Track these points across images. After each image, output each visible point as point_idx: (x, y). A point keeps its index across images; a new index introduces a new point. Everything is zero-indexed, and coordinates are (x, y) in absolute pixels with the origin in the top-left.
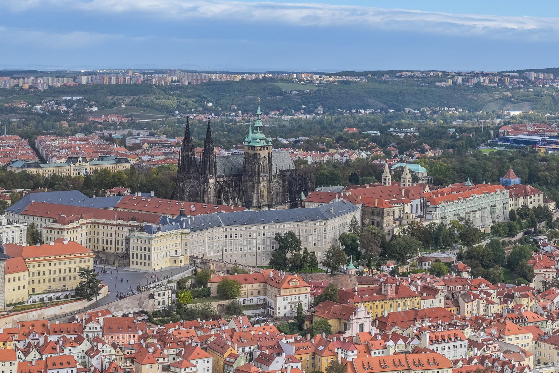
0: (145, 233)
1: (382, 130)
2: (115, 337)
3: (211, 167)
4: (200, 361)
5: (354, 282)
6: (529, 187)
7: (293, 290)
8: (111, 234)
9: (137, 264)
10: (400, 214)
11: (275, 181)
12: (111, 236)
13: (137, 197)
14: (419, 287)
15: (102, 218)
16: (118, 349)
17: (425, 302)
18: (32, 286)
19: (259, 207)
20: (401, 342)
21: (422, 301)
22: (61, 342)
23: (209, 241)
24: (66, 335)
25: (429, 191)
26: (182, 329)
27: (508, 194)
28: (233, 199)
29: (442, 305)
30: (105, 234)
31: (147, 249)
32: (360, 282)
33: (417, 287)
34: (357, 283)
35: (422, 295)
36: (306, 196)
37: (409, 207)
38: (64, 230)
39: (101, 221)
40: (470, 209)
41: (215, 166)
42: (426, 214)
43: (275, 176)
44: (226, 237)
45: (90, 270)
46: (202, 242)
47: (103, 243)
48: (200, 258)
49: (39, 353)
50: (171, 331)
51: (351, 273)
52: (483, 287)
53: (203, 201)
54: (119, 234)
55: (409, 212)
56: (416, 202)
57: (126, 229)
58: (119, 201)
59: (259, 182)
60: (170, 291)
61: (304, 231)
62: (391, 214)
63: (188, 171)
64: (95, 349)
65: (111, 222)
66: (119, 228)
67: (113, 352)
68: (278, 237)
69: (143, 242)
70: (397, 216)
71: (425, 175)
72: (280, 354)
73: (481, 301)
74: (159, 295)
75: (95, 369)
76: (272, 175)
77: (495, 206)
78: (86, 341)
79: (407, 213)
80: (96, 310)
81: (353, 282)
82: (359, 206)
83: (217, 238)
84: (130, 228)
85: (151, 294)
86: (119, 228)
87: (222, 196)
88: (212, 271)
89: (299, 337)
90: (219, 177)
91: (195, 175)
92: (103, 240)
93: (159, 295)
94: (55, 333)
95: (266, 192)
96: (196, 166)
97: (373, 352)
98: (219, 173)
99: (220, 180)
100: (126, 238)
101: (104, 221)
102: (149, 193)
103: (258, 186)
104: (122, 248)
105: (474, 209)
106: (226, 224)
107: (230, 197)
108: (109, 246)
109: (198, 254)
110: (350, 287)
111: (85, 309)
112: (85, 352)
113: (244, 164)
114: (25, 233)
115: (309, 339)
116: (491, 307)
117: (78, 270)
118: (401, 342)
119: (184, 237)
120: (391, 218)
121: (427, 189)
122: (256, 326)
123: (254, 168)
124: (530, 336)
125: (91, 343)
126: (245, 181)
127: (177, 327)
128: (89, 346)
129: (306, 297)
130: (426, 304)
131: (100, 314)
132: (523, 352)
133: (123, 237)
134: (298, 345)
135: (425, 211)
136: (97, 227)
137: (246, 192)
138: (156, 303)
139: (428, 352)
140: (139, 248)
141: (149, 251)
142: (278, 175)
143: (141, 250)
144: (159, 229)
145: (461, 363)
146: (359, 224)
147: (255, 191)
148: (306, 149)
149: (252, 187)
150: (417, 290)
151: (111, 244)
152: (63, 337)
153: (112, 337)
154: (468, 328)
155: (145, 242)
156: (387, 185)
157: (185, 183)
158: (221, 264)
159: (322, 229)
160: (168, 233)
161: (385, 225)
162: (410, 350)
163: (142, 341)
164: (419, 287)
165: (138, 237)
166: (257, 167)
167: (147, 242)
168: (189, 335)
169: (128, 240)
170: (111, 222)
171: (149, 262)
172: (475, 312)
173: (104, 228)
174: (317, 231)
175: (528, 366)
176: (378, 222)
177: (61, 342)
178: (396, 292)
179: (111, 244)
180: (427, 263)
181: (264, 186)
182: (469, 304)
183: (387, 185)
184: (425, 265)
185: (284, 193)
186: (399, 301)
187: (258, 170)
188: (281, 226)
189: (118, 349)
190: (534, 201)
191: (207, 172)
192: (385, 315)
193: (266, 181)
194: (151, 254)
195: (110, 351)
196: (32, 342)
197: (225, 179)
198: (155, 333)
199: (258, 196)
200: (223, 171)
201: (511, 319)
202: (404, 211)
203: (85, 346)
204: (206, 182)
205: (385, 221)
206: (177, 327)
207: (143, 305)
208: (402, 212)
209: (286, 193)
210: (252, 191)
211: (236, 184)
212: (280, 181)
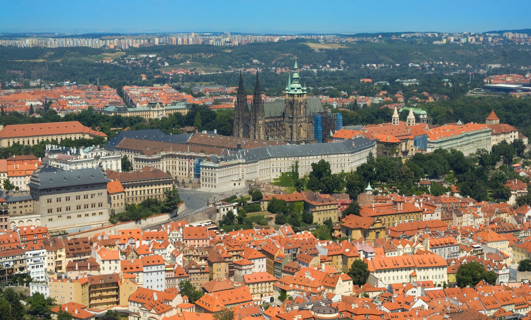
1: (392, 80)
2: (192, 242)
4: (257, 261)
5: (372, 200)
6: (507, 126)
7: (325, 207)
10: (406, 147)
14: (422, 204)
15: (178, 151)
16: (195, 251)
17: (425, 216)
19: (298, 143)
20: (408, 246)
21: (424, 215)
22: (152, 246)
24: (155, 240)
26: (242, 235)
29: (439, 218)
30: (181, 163)
31: (213, 175)
32: (376, 200)
33: (420, 204)
35: (424, 210)
39: (177, 153)
40: (461, 144)
47: (180, 170)
49: (137, 254)
50: (233, 236)
52: (471, 204)
58: (190, 137)
60: (232, 207)
68: (314, 165)
70: (403, 149)
71: (426, 116)
72: (316, 255)
73: (469, 215)
74: (224, 210)
75: (179, 266)
77: (481, 140)
78: (170, 245)
81: (371, 200)
85: (218, 209)
88: (263, 191)
89: (331, 242)
92: (180, 168)
94: (147, 239)
97: (387, 254)
99: (267, 121)
105: (464, 143)
108: (184, 171)
110: (368, 205)
112: (170, 252)
114: (120, 162)
115: (338, 243)
116: (476, 220)
118: (408, 246)
122: (298, 233)
124: (508, 243)
127: (238, 234)
128: (173, 248)
129: (335, 212)
130: (427, 218)
132: (502, 254)
134: (330, 248)
139: (429, 254)
144: (222, 160)
145: (453, 262)
146: (375, 156)
148: (332, 96)
151: (185, 171)
152: (154, 241)
154: (460, 236)
156: (396, 124)
162: (415, 252)
168: (247, 240)
172: (464, 224)
175: (506, 265)
177: (152, 246)
178: (404, 208)
179: (185, 171)
182: (460, 218)
190: (511, 137)
196: (131, 245)
198: (222, 239)
201: (493, 229)
203: (171, 249)
206: (238, 234)
207: (212, 217)
208: (408, 146)
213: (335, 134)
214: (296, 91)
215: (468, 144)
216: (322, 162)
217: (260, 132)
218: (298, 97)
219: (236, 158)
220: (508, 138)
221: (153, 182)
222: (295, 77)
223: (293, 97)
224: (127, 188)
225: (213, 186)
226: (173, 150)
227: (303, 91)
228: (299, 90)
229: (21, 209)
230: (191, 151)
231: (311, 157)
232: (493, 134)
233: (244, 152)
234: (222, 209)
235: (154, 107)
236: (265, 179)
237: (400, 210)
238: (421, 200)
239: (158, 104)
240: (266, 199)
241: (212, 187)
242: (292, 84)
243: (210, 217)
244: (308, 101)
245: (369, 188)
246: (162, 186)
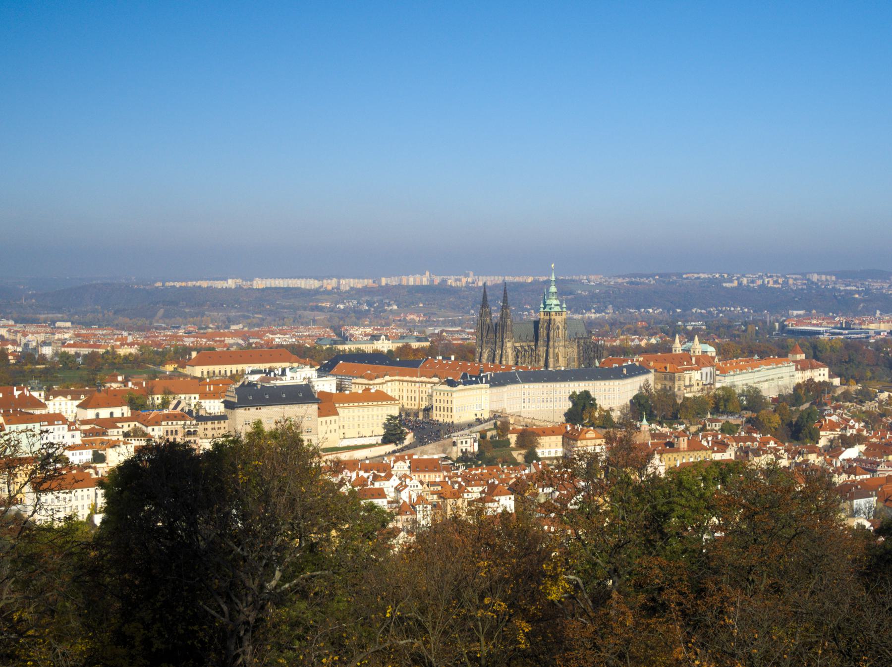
10: (690, 381)
13: (439, 360)
14: (710, 443)
16: (425, 485)
18: (342, 431)
22: (371, 478)
27: (794, 367)
29: (733, 457)
31: (449, 402)
33: (708, 443)
52: (772, 444)
55: (700, 379)
56: (705, 370)
57: (429, 386)
61: (598, 390)
62: (682, 379)
63: (487, 336)
64: (404, 484)
65: (415, 379)
67: (420, 487)
70: (687, 383)
74: (462, 442)
75: (405, 502)
77: (782, 377)
78: (394, 477)
80: (403, 453)
85: (454, 442)
93: (462, 442)
94: (366, 471)
99: (517, 345)
105: (762, 379)
108: (413, 402)
111: (394, 452)
120: (682, 382)
121: (716, 360)
125: (400, 479)
131: (406, 457)
138: (459, 450)
150: (708, 443)
152: (374, 473)
153: (419, 476)
160: (468, 387)
161: (676, 390)
163: (447, 479)
164: (710, 443)
165: (440, 390)
167: (450, 394)
169: (430, 396)
174: (612, 390)
176: (670, 387)
180: (717, 424)
183: (677, 352)
184: (716, 426)
185: (579, 358)
186: (691, 454)
189: (425, 485)
190: (820, 375)
192: (678, 465)
195: (417, 486)
203: (395, 481)
205: (676, 386)
206: (480, 470)
212: (575, 347)
215: (767, 380)
217: (507, 357)
219: (476, 382)
220: (816, 376)
227: (562, 308)
229: (214, 432)
232: (797, 369)
233: (487, 376)
234: (459, 441)
235: (378, 340)
238: (710, 439)
239: (383, 337)
243: (444, 451)
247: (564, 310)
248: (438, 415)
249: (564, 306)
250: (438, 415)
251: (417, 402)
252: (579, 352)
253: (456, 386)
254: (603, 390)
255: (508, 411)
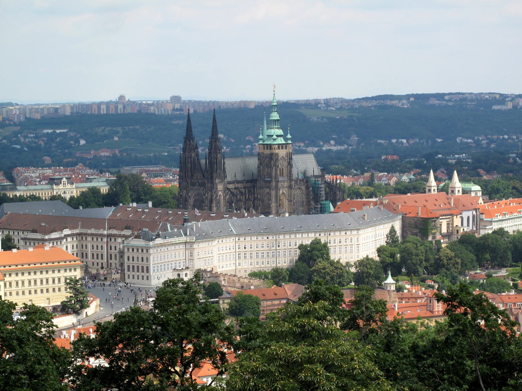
0: (142, 240)
3: (219, 169)
5: (394, 299)
8: (102, 247)
9: (133, 278)
10: (448, 227)
11: (296, 187)
12: (102, 249)
13: (132, 207)
15: (90, 228)
23: (219, 253)
25: (483, 203)
28: (248, 210)
30: (95, 247)
31: (145, 259)
34: (397, 300)
36: (334, 207)
37: (460, 220)
38: (46, 240)
41: (224, 169)
42: (479, 229)
43: (296, 181)
44: (239, 248)
45: (77, 278)
46: (210, 253)
47: (93, 258)
48: (208, 272)
51: (390, 288)
53: (211, 209)
54: (111, 247)
55: (460, 225)
57: (119, 240)
59: (277, 188)
63: (192, 176)
65: (101, 232)
66: (111, 239)
68: (301, 247)
69: (140, 251)
70: (444, 230)
76: (292, 180)
79: (457, 226)
81: (392, 299)
82: (400, 217)
83: (228, 248)
84: (124, 239)
86: (111, 239)
87: (233, 205)
88: (224, 286)
90: (229, 183)
91: (200, 181)
92: (93, 254)
95: (287, 201)
96: (202, 170)
98: (229, 178)
99: (231, 186)
100: (120, 250)
101: (92, 231)
102: (146, 204)
103: (276, 193)
104: (116, 264)
106: (238, 235)
107: (243, 207)
108: (100, 261)
109: (206, 267)
113: (258, 167)
117: (63, 280)
119: (188, 246)
121: (481, 201)
123: (271, 171)
126: (261, 188)
133: (116, 249)
135: (477, 221)
136: (84, 239)
137: (263, 201)
140: (135, 259)
141: (147, 262)
142: (301, 180)
143: (138, 261)
144: (158, 236)
147: (273, 199)
149: (269, 194)
155: (142, 250)
157: (189, 190)
158: (234, 278)
159: (354, 239)
166: (274, 170)
167: (145, 251)
170: (101, 232)
171: (147, 274)
173: (93, 239)
179: (102, 259)
181: (283, 193)
187: (276, 174)
188: (305, 235)
191: (214, 176)
193: (286, 187)
194: (150, 265)
197: (237, 186)
199: (277, 206)
200: (234, 176)
202: (452, 224)
204: (213, 188)
208: (451, 226)
209: (310, 202)
210: (270, 199)
211: (249, 191)
212: (303, 188)
213: (336, 207)
214: (275, 140)
216: (316, 243)
217: (218, 202)
218: (279, 148)
221: (50, 266)
222: (274, 118)
223: (271, 149)
224: (7, 276)
225: (145, 278)
226: (82, 228)
227: (286, 139)
228: (279, 138)
230: (110, 228)
231: (299, 236)
233: (192, 225)
235: (57, 184)
236: (226, 269)
237: (438, 312)
239: (64, 179)
240: (228, 296)
241: (143, 279)
242: (269, 130)
244: (294, 157)
245: (390, 280)
246: (63, 274)
247: (290, 142)
248: (131, 277)
249: (289, 136)
250: (131, 277)
251: (105, 260)
252: (308, 194)
253: (152, 240)
254: (337, 240)
255: (219, 270)
